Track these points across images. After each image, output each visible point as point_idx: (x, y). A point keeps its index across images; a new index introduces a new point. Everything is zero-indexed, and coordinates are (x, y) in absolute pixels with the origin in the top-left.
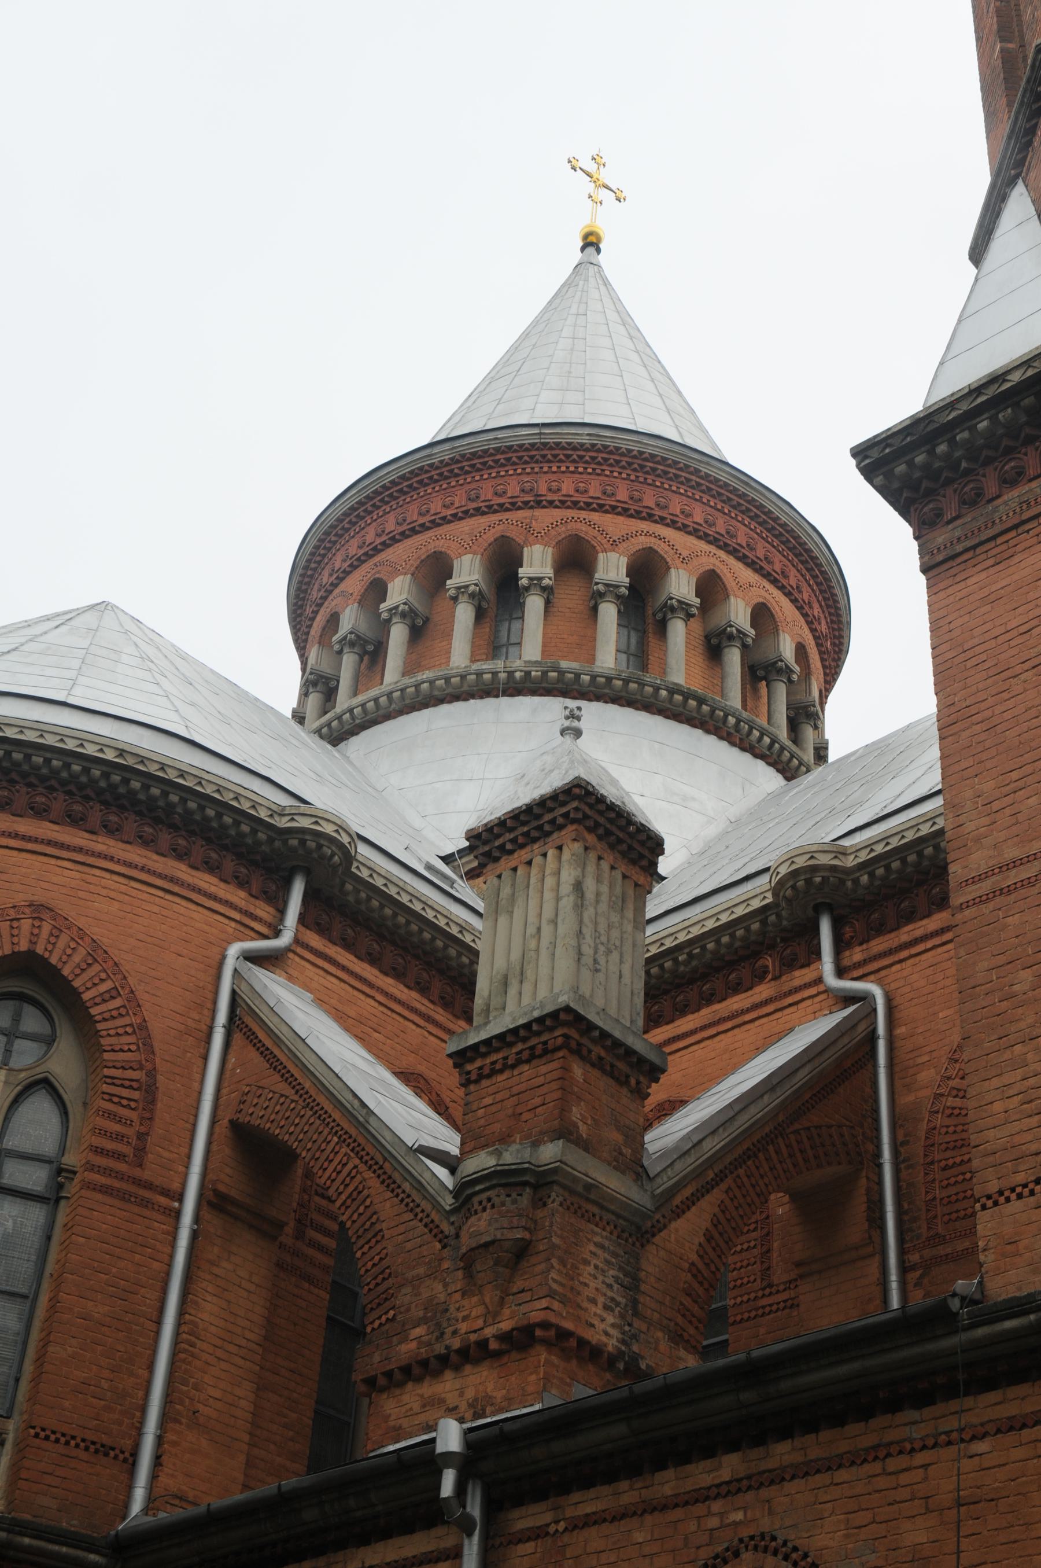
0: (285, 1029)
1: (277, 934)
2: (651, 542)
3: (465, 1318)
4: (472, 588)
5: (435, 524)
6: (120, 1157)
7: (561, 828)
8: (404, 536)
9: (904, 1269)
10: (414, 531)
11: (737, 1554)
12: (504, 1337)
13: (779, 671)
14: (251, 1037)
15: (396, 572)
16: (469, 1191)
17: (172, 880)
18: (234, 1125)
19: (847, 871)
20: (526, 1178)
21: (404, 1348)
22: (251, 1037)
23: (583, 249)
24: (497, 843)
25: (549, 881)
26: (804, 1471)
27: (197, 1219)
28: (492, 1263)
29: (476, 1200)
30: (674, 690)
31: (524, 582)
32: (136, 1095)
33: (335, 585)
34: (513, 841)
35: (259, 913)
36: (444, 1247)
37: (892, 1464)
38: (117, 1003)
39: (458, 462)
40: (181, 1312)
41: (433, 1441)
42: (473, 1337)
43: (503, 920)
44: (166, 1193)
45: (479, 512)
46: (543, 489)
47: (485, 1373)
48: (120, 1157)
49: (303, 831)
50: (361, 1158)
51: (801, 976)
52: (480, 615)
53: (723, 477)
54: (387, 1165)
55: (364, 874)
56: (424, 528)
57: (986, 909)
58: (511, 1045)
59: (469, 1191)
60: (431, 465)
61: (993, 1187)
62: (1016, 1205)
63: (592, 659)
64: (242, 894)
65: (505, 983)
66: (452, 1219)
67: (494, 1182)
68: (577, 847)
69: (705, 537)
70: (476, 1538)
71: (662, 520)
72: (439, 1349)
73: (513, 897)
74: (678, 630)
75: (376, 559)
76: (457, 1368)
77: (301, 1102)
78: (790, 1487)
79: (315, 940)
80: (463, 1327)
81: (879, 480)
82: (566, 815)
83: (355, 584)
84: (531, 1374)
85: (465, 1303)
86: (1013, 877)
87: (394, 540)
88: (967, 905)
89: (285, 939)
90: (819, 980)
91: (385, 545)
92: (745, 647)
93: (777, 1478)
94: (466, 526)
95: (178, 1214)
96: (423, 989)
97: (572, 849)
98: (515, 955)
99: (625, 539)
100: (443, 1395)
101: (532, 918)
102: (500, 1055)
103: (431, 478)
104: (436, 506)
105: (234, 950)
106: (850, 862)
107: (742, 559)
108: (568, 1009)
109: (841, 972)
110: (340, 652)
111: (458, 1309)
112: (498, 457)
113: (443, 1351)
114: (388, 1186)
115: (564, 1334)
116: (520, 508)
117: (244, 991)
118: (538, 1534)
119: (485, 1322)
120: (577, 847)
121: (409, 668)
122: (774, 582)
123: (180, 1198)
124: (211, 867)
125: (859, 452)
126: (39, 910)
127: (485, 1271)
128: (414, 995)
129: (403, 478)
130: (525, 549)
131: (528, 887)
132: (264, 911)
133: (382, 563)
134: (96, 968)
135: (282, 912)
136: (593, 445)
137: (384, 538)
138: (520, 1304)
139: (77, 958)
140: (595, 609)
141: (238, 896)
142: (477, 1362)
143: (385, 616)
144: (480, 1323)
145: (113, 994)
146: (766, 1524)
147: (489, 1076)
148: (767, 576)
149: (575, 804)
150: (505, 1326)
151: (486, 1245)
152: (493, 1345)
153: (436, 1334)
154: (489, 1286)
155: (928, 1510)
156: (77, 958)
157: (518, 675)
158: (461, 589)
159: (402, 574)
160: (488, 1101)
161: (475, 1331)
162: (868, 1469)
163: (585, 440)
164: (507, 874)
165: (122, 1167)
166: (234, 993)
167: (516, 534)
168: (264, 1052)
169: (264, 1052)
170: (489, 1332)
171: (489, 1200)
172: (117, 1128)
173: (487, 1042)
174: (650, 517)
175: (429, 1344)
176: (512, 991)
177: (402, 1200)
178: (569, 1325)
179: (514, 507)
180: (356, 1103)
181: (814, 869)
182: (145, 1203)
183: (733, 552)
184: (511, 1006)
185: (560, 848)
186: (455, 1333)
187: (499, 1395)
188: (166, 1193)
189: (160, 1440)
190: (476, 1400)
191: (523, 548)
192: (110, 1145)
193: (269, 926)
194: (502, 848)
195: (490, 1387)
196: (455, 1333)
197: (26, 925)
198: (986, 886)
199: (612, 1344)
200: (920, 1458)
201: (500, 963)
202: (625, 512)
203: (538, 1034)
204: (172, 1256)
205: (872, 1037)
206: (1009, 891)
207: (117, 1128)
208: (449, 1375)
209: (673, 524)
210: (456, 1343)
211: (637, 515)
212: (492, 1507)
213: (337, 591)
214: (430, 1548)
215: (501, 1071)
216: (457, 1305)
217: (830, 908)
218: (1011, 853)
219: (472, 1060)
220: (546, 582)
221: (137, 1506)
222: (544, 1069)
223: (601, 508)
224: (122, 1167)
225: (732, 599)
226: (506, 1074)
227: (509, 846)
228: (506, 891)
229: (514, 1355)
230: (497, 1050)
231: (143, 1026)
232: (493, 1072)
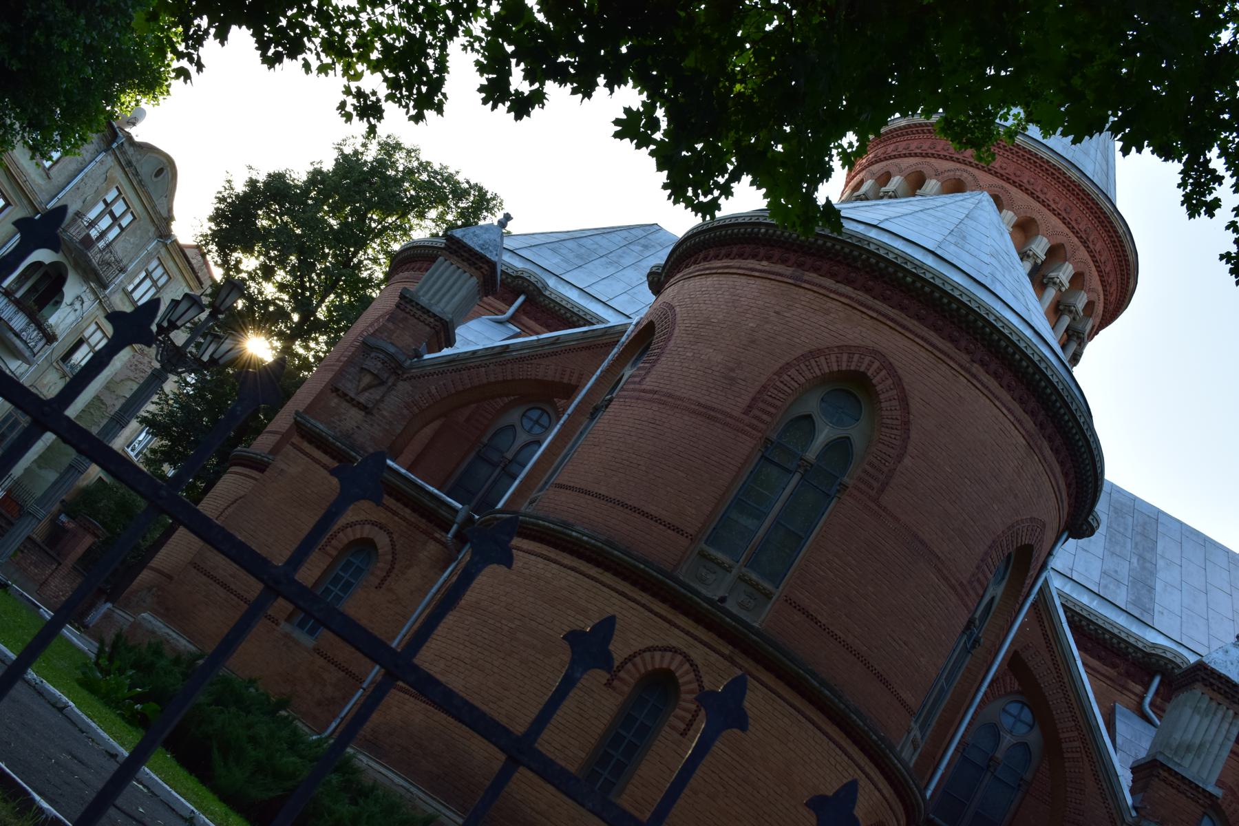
5: (1043, 203)
8: (1026, 191)
14: (1041, 622)
15: (1011, 209)
22: (1041, 622)
24: (1211, 680)
25: (1226, 726)
34: (1220, 688)
39: (1075, 185)
45: (1063, 220)
46: (1091, 239)
50: (1084, 747)
54: (1097, 764)
56: (1037, 199)
58: (1185, 784)
60: (1065, 173)
75: (1006, 185)
77: (1060, 684)
102: (1177, 782)
103: (1058, 178)
104: (1051, 195)
112: (1089, 202)
114: (1094, 775)
116: (1077, 237)
129: (1048, 162)
131: (1215, 714)
133: (1007, 191)
136: (1120, 237)
137: (1017, 180)
159: (1013, 211)
160: (1163, 794)
163: (1120, 231)
164: (1207, 698)
167: (1068, 248)
169: (1045, 635)
173: (1177, 773)
176: (1190, 756)
177: (1099, 789)
179: (1076, 233)
184: (1186, 763)
194: (1212, 685)
201: (1189, 736)
215: (1173, 788)
227: (1216, 688)
230: (1178, 779)
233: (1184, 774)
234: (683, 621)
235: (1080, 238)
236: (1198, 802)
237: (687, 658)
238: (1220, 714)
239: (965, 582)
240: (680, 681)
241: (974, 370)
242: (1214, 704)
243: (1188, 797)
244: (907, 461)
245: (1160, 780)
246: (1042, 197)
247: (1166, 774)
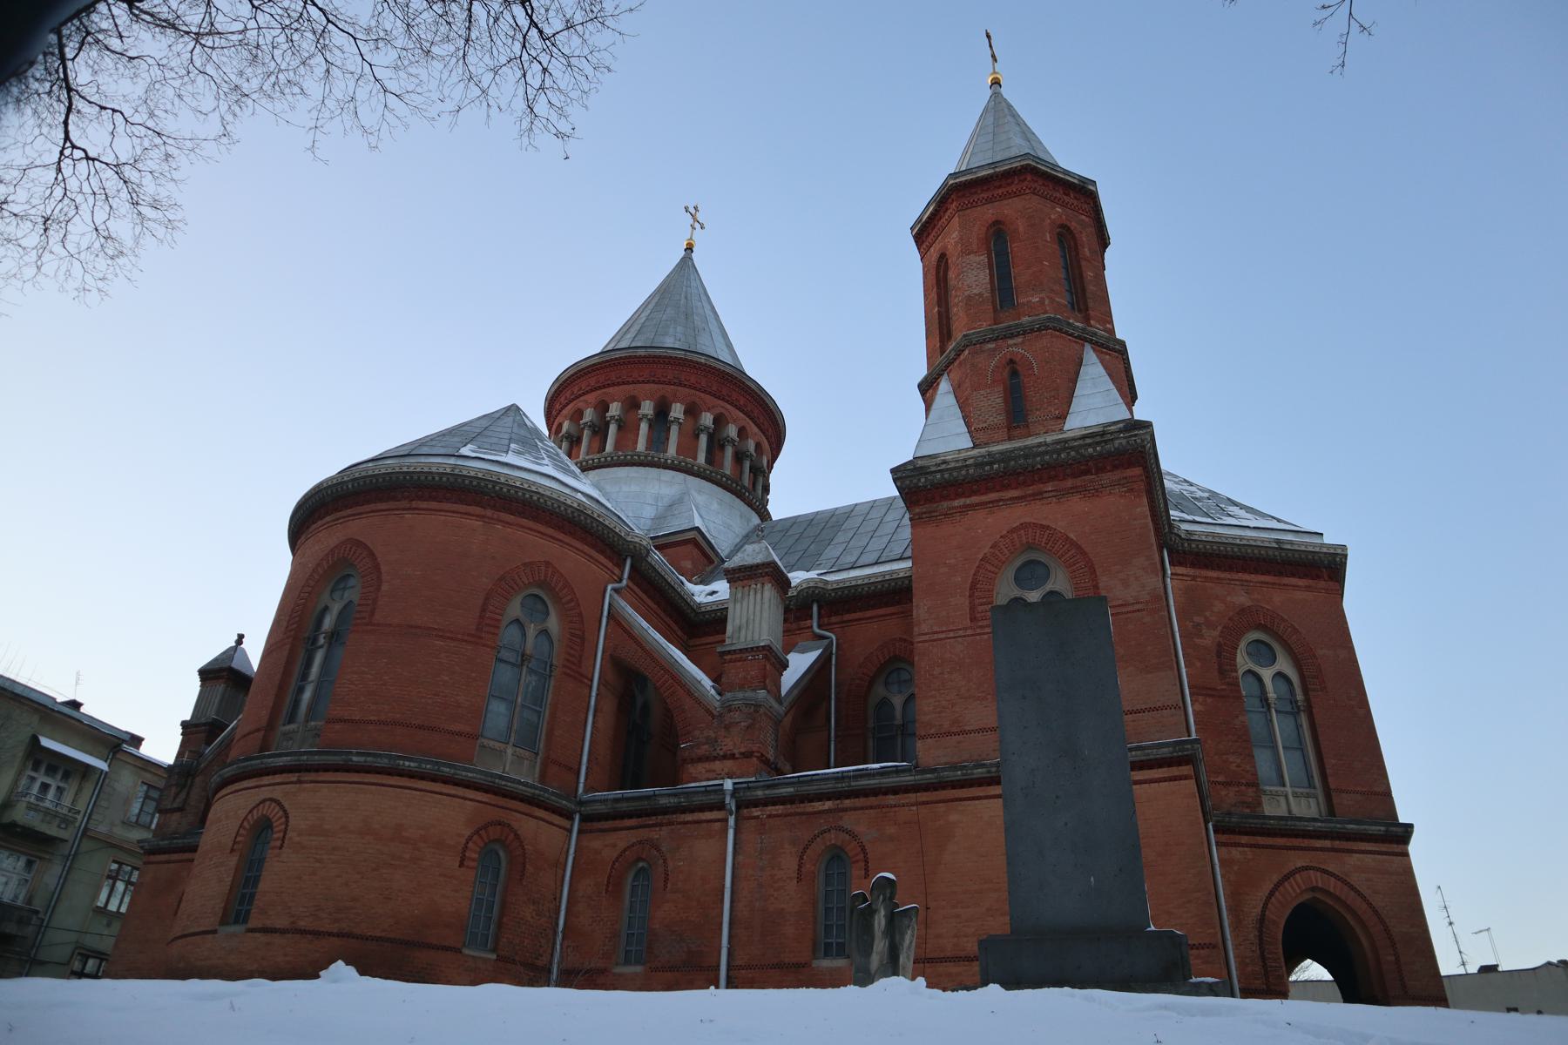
0: (636, 624)
1: (620, 580)
2: (723, 411)
4: (649, 417)
5: (633, 383)
6: (574, 664)
7: (763, 577)
8: (618, 384)
9: (836, 737)
10: (624, 383)
11: (829, 830)
12: (741, 754)
13: (761, 472)
17: (591, 557)
18: (611, 655)
19: (828, 590)
20: (753, 702)
21: (699, 751)
22: (619, 624)
23: (685, 250)
25: (759, 596)
26: (855, 809)
27: (598, 689)
30: (724, 475)
31: (672, 419)
32: (579, 640)
33: (581, 396)
34: (744, 576)
35: (615, 572)
37: (884, 810)
38: (573, 604)
40: (594, 723)
41: (722, 785)
42: (729, 752)
43: (738, 605)
44: (587, 678)
45: (654, 382)
48: (574, 664)
49: (636, 542)
51: (802, 623)
52: (650, 426)
53: (753, 387)
55: (649, 559)
56: (628, 383)
57: (927, 644)
61: (923, 734)
62: (929, 740)
63: (695, 458)
64: (611, 564)
65: (740, 628)
68: (770, 585)
69: (742, 411)
70: (733, 816)
71: (727, 402)
72: (715, 754)
73: (742, 598)
74: (729, 451)
78: (849, 813)
79: (631, 584)
80: (725, 748)
81: (899, 484)
82: (767, 573)
83: (591, 398)
86: (936, 636)
87: (614, 385)
88: (920, 642)
89: (625, 582)
90: (812, 627)
91: (609, 386)
92: (752, 460)
93: (845, 810)
94: (647, 386)
95: (591, 687)
96: (657, 603)
97: (768, 587)
98: (744, 620)
99: (713, 407)
101: (751, 607)
105: (609, 587)
106: (829, 587)
107: (755, 423)
108: (769, 646)
109: (820, 627)
110: (583, 429)
115: (762, 755)
117: (615, 605)
118: (758, 817)
120: (770, 585)
121: (617, 446)
122: (764, 433)
123: (592, 681)
124: (602, 552)
125: (893, 471)
126: (548, 564)
128: (656, 606)
129: (621, 358)
130: (673, 405)
132: (617, 571)
134: (566, 589)
135: (623, 572)
139: (560, 585)
140: (697, 436)
141: (610, 565)
143: (609, 419)
144: (732, 748)
145: (572, 600)
146: (840, 823)
148: (761, 430)
149: (771, 569)
150: (743, 750)
152: (737, 756)
155: (895, 824)
156: (560, 585)
157: (669, 461)
158: (645, 416)
162: (876, 811)
163: (703, 361)
164: (740, 589)
165: (574, 667)
166: (610, 604)
168: (626, 631)
170: (736, 751)
172: (572, 652)
173: (735, 650)
174: (723, 400)
178: (764, 753)
179: (670, 383)
180: (673, 660)
181: (816, 587)
182: (582, 682)
183: (751, 419)
185: (763, 584)
186: (721, 749)
188: (587, 678)
189: (587, 768)
191: (671, 405)
192: (571, 659)
193: (618, 577)
196: (721, 749)
197: (543, 568)
198: (926, 638)
199: (772, 759)
200: (894, 809)
201: (737, 622)
202: (714, 395)
204: (589, 702)
205: (831, 653)
206: (935, 640)
207: (572, 652)
208: (717, 762)
209: (731, 404)
210: (721, 753)
211: (719, 398)
212: (738, 807)
213: (582, 398)
217: (818, 602)
219: (727, 655)
220: (681, 421)
221: (581, 790)
223: (705, 392)
224: (574, 667)
225: (749, 440)
228: (739, 595)
231: (580, 615)
232: (735, 661)
234: (266, 780)
235: (674, 384)
237: (272, 800)
238: (752, 593)
239: (473, 632)
240: (271, 817)
241: (414, 506)
242: (746, 589)
244: (385, 587)
246: (630, 380)
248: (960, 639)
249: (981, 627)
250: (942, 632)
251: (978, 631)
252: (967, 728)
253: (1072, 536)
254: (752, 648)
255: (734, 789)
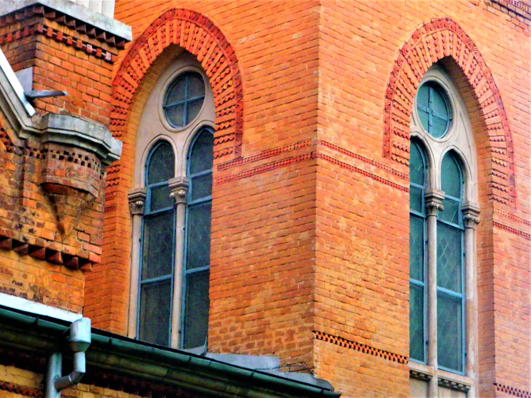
3: (40, 225)
16: (76, 143)
28: (79, 205)
29: (77, 152)
36: (9, 151)
42: (47, 244)
47: (43, 271)
59: (76, 143)
66: (22, 135)
67: (95, 150)
72: (18, 236)
76: (21, 254)
80: (39, 231)
84: (76, 290)
85: (39, 212)
86: (343, 159)
100: (10, 269)
111: (34, 214)
113: (21, 240)
119: (55, 238)
127: (72, 207)
138: (81, 240)
142: (38, 258)
144: (51, 236)
147: (58, 41)
150: (72, 250)
151: (81, 191)
153: (15, 223)
154: (71, 218)
160: (58, 61)
161: (48, 240)
170: (59, 247)
171: (87, 158)
173: (69, 18)
175: (9, 226)
186: (31, 231)
187: (54, 293)
190: (35, 286)
195: (46, 282)
196: (31, 231)
203: (102, 41)
206: (343, 165)
208: (13, 255)
210: (32, 241)
214: (7, 380)
215: (68, 45)
216: (33, 211)
218: (344, 144)
222: (99, 70)
226: (70, 50)
229: (63, 269)
230: (71, 28)
232: (65, 42)
233: (79, 18)
236: (103, 58)
243: (88, 54)
245: (48, 37)
247: (54, 25)
248: (371, 181)
249: (395, 173)
250: (351, 155)
251: (392, 179)
252: (373, 344)
253: (496, 79)
254: (99, 31)
255: (93, 340)
